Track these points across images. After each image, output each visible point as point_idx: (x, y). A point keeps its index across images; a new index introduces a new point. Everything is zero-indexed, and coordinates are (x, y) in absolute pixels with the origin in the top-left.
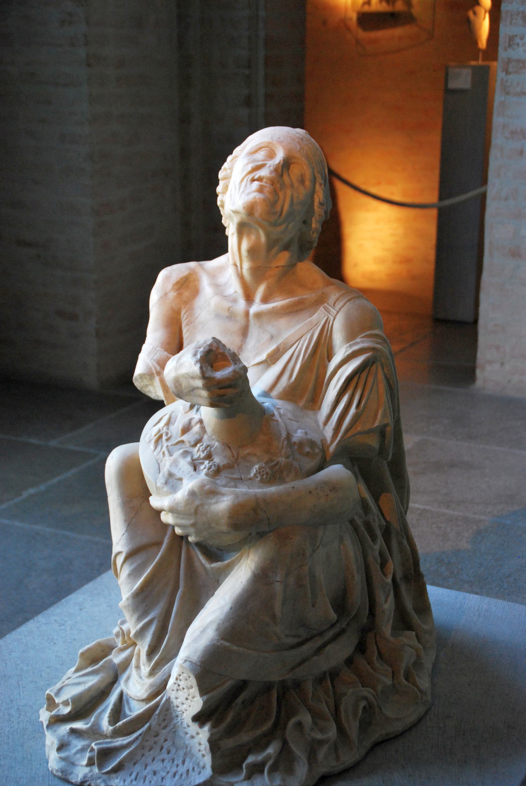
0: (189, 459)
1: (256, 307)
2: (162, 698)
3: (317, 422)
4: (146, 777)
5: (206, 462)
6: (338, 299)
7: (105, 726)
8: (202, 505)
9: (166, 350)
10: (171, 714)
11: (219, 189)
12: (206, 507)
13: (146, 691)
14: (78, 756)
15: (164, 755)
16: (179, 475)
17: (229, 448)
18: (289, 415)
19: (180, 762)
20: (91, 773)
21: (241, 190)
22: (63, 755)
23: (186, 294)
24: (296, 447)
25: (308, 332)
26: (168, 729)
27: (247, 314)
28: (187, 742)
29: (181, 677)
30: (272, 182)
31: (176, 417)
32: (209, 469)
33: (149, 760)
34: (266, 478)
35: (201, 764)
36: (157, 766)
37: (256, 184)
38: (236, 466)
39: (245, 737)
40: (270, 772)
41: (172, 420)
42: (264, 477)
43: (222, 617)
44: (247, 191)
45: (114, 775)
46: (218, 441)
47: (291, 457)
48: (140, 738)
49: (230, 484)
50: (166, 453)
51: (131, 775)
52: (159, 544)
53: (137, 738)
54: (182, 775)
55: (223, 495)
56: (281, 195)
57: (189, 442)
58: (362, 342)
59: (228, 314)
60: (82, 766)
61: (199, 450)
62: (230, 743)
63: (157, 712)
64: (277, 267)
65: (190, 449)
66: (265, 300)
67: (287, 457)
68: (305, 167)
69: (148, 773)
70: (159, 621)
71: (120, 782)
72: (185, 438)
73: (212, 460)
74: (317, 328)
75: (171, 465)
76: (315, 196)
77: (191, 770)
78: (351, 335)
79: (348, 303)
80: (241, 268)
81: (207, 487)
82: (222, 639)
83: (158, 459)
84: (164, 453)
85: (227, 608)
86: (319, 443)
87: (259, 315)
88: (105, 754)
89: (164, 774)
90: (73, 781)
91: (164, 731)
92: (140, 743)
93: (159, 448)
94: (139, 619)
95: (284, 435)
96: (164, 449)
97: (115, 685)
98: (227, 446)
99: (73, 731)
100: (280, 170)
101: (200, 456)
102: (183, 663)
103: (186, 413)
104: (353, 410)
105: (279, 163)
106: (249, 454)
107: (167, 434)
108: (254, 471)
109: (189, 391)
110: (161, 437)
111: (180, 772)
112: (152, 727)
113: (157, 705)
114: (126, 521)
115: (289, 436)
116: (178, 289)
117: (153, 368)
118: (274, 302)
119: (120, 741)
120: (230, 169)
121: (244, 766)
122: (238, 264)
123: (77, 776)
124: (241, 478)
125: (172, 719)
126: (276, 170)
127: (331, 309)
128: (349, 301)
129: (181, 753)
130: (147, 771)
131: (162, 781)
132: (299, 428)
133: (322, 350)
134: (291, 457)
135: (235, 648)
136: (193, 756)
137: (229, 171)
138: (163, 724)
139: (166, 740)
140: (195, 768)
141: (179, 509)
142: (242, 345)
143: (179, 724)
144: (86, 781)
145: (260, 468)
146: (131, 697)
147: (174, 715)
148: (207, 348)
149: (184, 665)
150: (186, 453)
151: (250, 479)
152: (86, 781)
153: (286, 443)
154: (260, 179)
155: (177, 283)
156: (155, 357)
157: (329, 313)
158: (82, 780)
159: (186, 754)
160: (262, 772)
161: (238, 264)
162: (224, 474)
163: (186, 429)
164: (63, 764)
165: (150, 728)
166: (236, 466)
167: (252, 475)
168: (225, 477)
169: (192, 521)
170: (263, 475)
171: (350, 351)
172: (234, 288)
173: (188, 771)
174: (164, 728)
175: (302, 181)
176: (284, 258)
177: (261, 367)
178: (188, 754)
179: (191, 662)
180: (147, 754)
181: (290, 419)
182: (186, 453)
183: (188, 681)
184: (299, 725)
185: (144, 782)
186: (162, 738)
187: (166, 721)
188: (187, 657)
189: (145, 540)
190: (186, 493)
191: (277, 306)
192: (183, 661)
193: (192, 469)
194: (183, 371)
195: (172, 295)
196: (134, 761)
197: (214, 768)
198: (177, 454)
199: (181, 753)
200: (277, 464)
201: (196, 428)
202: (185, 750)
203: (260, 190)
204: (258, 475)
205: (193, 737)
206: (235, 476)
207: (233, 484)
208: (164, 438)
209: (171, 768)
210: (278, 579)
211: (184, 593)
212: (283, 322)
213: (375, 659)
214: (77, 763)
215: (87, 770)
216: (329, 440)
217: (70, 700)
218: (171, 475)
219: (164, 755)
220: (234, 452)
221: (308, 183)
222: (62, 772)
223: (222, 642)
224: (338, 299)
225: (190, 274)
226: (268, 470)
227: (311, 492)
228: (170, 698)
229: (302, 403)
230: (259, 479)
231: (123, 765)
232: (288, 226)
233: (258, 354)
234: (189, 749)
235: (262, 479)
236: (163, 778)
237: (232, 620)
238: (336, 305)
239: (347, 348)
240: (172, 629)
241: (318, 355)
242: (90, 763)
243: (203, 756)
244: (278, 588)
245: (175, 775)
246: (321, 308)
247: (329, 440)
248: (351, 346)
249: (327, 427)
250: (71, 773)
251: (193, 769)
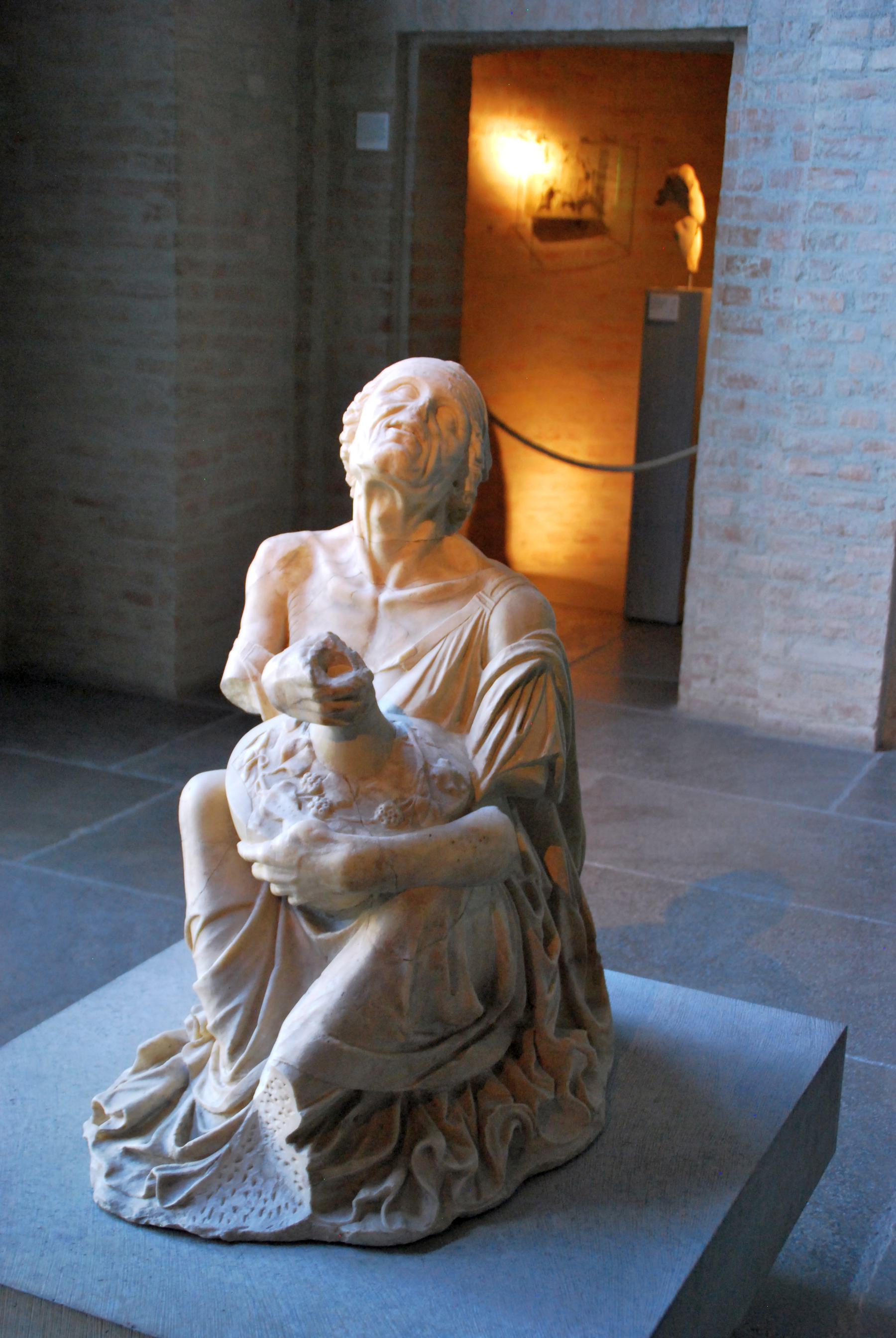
0: (292, 793)
1: (389, 594)
2: (247, 1111)
3: (464, 749)
4: (222, 1214)
5: (315, 798)
6: (496, 587)
7: (171, 1146)
8: (308, 855)
9: (267, 647)
10: (259, 1132)
11: (343, 437)
12: (313, 858)
13: (227, 1100)
14: (134, 1184)
15: (248, 1186)
16: (278, 814)
17: (347, 780)
18: (429, 739)
19: (269, 1196)
21: (373, 438)
22: (114, 1182)
23: (296, 573)
24: (436, 782)
25: (455, 629)
26: (254, 1153)
27: (376, 602)
28: (279, 1170)
29: (273, 1084)
30: (414, 429)
31: (277, 737)
32: (319, 807)
33: (228, 1192)
34: (395, 822)
35: (297, 1200)
36: (238, 1200)
37: (392, 432)
38: (354, 804)
39: (357, 1165)
40: (389, 1211)
41: (271, 741)
42: (392, 820)
44: (381, 440)
45: (181, 1211)
46: (332, 770)
47: (429, 795)
48: (217, 1163)
49: (345, 829)
50: (262, 785)
51: (202, 1211)
52: (249, 906)
53: (212, 1163)
54: (270, 1213)
55: (336, 842)
56: (425, 446)
57: (293, 771)
58: (527, 644)
60: (138, 1198)
61: (306, 782)
62: (336, 1173)
63: (240, 1129)
64: (418, 541)
65: (294, 780)
66: (401, 584)
67: (423, 795)
68: (458, 412)
69: (226, 1210)
70: (246, 1009)
71: (188, 1220)
72: (288, 765)
73: (323, 796)
74: (468, 623)
75: (268, 802)
76: (471, 450)
77: (283, 1206)
78: (513, 636)
79: (510, 592)
80: (370, 542)
81: (315, 832)
82: (330, 1035)
84: (258, 785)
85: (337, 995)
86: (466, 776)
87: (391, 605)
88: (169, 1184)
89: (247, 1211)
90: (126, 1217)
91: (250, 1155)
92: (217, 1170)
93: (252, 778)
94: (220, 1005)
95: (420, 765)
96: (260, 779)
97: (186, 1093)
98: (343, 777)
99: (128, 1152)
100: (424, 414)
101: (306, 790)
103: (290, 732)
104: (513, 734)
105: (424, 405)
106: (373, 789)
107: (264, 759)
108: (378, 812)
109: (295, 703)
110: (255, 763)
112: (233, 1150)
113: (240, 1121)
114: (205, 874)
115: (426, 768)
116: (286, 566)
117: (248, 671)
118: (413, 587)
120: (358, 410)
121: (354, 1202)
122: (366, 535)
123: (132, 1210)
124: (361, 822)
125: (260, 1139)
126: (419, 414)
127: (488, 599)
128: (511, 589)
129: (271, 1184)
130: (224, 1206)
131: (244, 1220)
132: (441, 756)
133: (473, 653)
134: (429, 795)
135: (346, 1047)
136: (286, 1189)
137: (357, 414)
138: (248, 1146)
139: (251, 1167)
140: (290, 1205)
141: (277, 860)
142: (367, 643)
143: (269, 1146)
144: (143, 1218)
145: (387, 808)
147: (262, 1133)
148: (321, 646)
149: (278, 1068)
150: (289, 785)
151: (373, 822)
152: (143, 1218)
153: (422, 775)
154: (398, 426)
155: (284, 559)
156: (250, 657)
157: (484, 604)
158: (138, 1216)
159: (276, 1186)
160: (377, 1211)
161: (366, 535)
162: (338, 815)
163: (289, 754)
164: (113, 1195)
165: (229, 1150)
166: (354, 804)
167: (376, 817)
168: (340, 819)
169: (293, 877)
170: (390, 818)
171: (511, 656)
172: (360, 567)
173: (279, 1208)
174: (250, 1150)
175: (454, 430)
176: (427, 530)
177: (393, 672)
178: (280, 1185)
180: (226, 1184)
181: (428, 744)
182: (289, 785)
183: (283, 1090)
184: (429, 1150)
185: (220, 1221)
186: (245, 1164)
187: (252, 1142)
189: (230, 901)
190: (287, 839)
191: (415, 594)
192: (276, 1063)
193: (296, 806)
194: (288, 675)
195: (277, 574)
196: (208, 1193)
197: (314, 1205)
198: (276, 786)
199: (271, 1184)
200: (410, 802)
201: (303, 753)
202: (276, 1181)
203: (398, 439)
204: (384, 818)
205: (287, 1164)
206: (353, 818)
207: (350, 828)
208: (260, 764)
209: (257, 1202)
210: (407, 956)
211: (280, 973)
212: (423, 614)
213: (533, 1067)
214: (132, 1193)
215: (145, 1203)
216: (480, 772)
217: (124, 1111)
218: (267, 814)
219: (248, 1186)
220: (353, 786)
221: (461, 432)
222: (112, 1204)
223: (330, 1038)
224: (496, 587)
225: (301, 548)
226: (397, 811)
227: (453, 842)
228: (257, 1112)
229: (445, 723)
230: (385, 822)
231: (192, 1198)
232: (432, 489)
233: (389, 655)
234: (280, 1180)
235: (389, 823)
236: (245, 1217)
237: (343, 1010)
238: (494, 594)
239: (507, 651)
240: (263, 1020)
241: (469, 659)
242: (150, 1194)
243: (300, 1188)
244: (406, 968)
245: (261, 1213)
246: (475, 598)
247: (480, 772)
248: (512, 649)
249: (477, 757)
250: (123, 1207)
251: (287, 1205)
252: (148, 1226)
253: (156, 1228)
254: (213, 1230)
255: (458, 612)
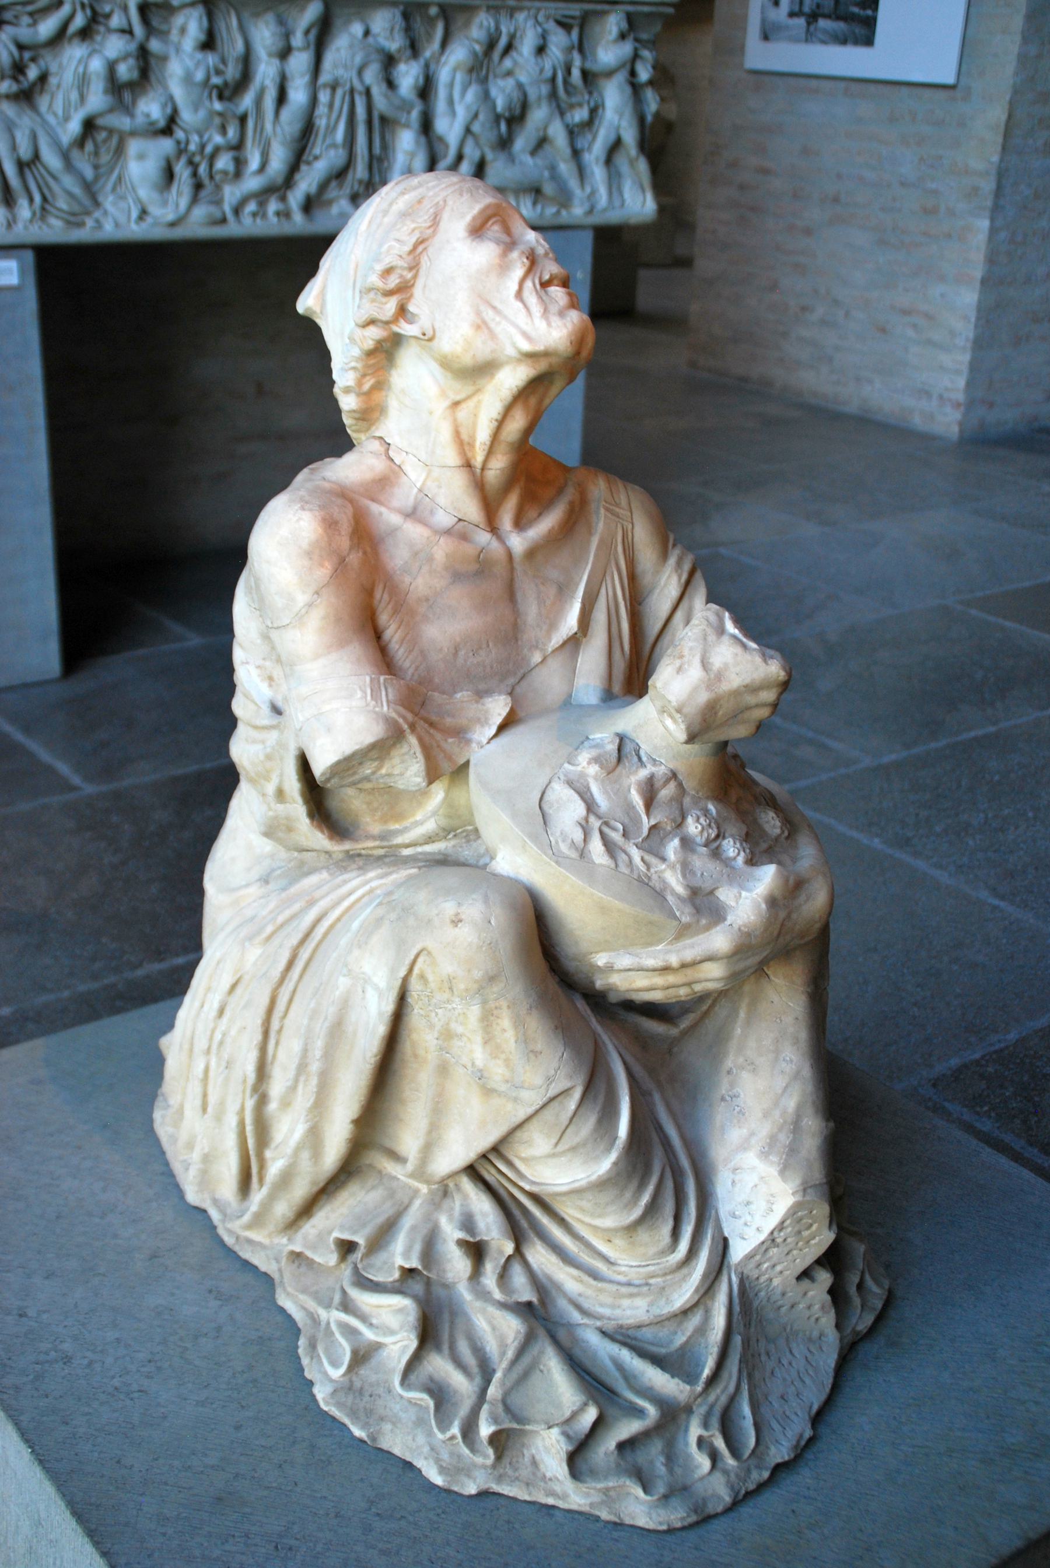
12: (794, 916)
16: (707, 886)
20: (732, 1475)
25: (609, 561)
26: (753, 1323)
43: (810, 1088)
53: (740, 1371)
59: (478, 566)
60: (702, 1479)
75: (684, 876)
83: (639, 876)
87: (531, 553)
99: (621, 1446)
102: (804, 1196)
103: (609, 773)
111: (802, 1369)
117: (401, 721)
119: (720, 1395)
123: (720, 1498)
142: (516, 620)
146: (639, 1327)
152: (738, 1493)
157: (618, 517)
159: (787, 1340)
161: (479, 459)
164: (675, 1501)
171: (685, 577)
179: (815, 1186)
188: (802, 1184)
194: (734, 680)
199: (781, 1342)
202: (784, 1334)
222: (696, 1511)
234: (788, 1330)
252: (749, 1494)
253: (761, 1487)
254: (801, 1436)
255: (595, 541)
